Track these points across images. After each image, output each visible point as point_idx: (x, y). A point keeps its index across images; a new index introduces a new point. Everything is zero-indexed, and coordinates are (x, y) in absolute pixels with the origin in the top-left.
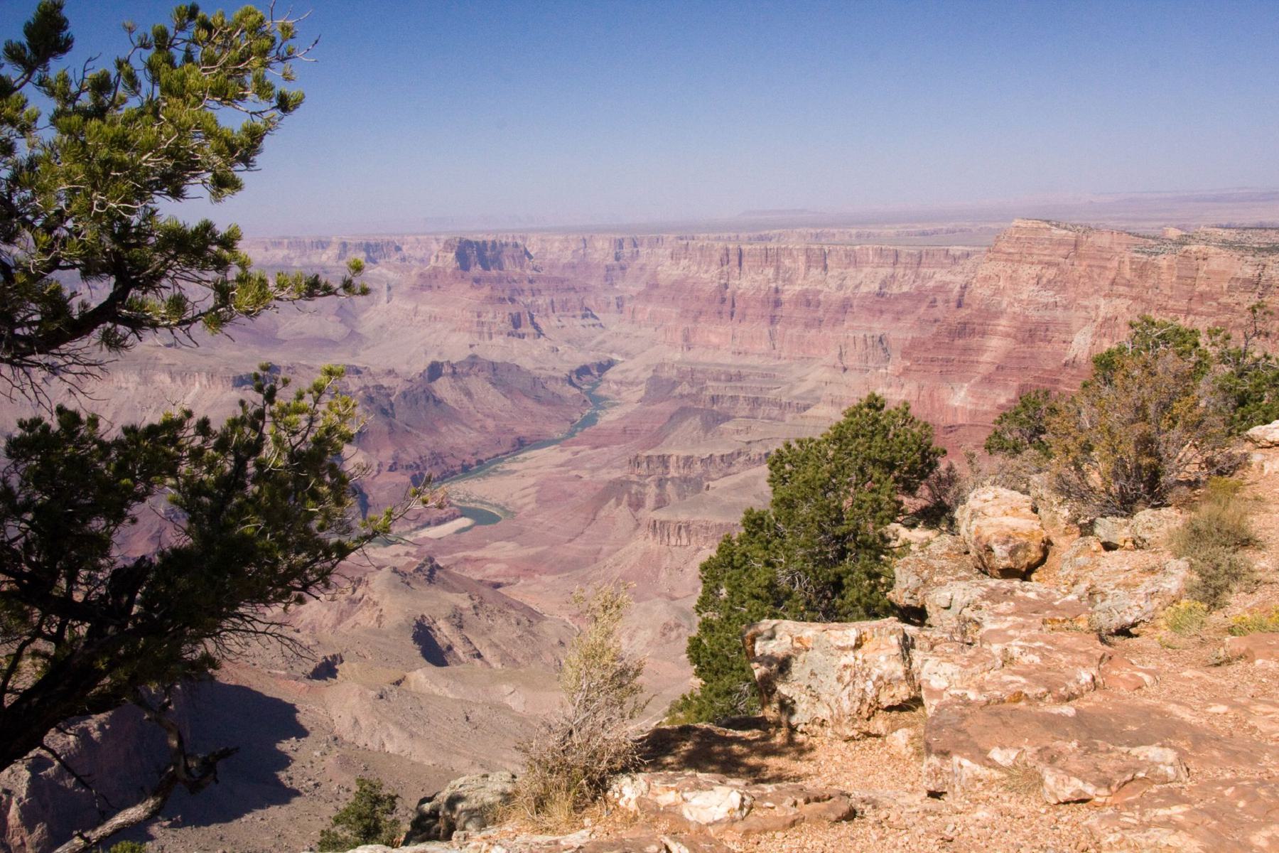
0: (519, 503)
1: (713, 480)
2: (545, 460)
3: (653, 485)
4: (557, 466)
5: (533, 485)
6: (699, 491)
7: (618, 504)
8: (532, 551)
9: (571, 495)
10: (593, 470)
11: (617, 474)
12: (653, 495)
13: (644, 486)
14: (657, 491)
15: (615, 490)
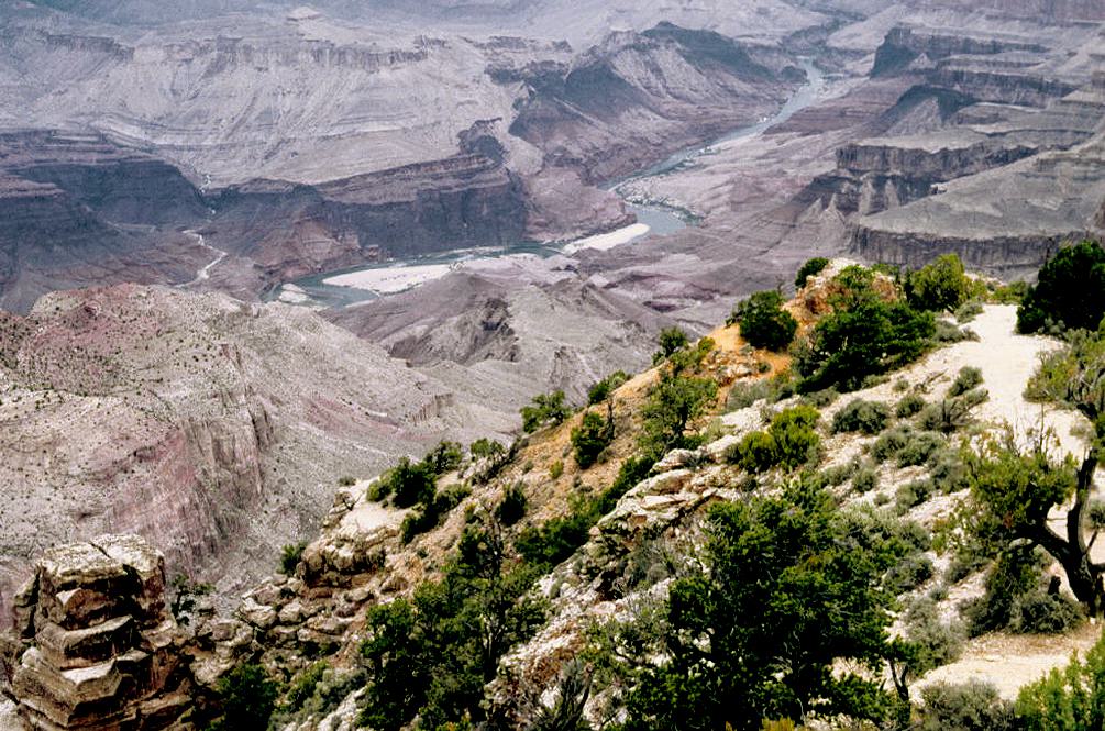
0: (708, 204)
1: (942, 182)
2: (743, 147)
3: (870, 186)
4: (759, 158)
5: (727, 183)
6: (926, 195)
7: (825, 205)
8: (714, 266)
9: (772, 196)
10: (802, 163)
11: (829, 167)
12: (868, 197)
13: (858, 184)
14: (874, 192)
15: (822, 187)
